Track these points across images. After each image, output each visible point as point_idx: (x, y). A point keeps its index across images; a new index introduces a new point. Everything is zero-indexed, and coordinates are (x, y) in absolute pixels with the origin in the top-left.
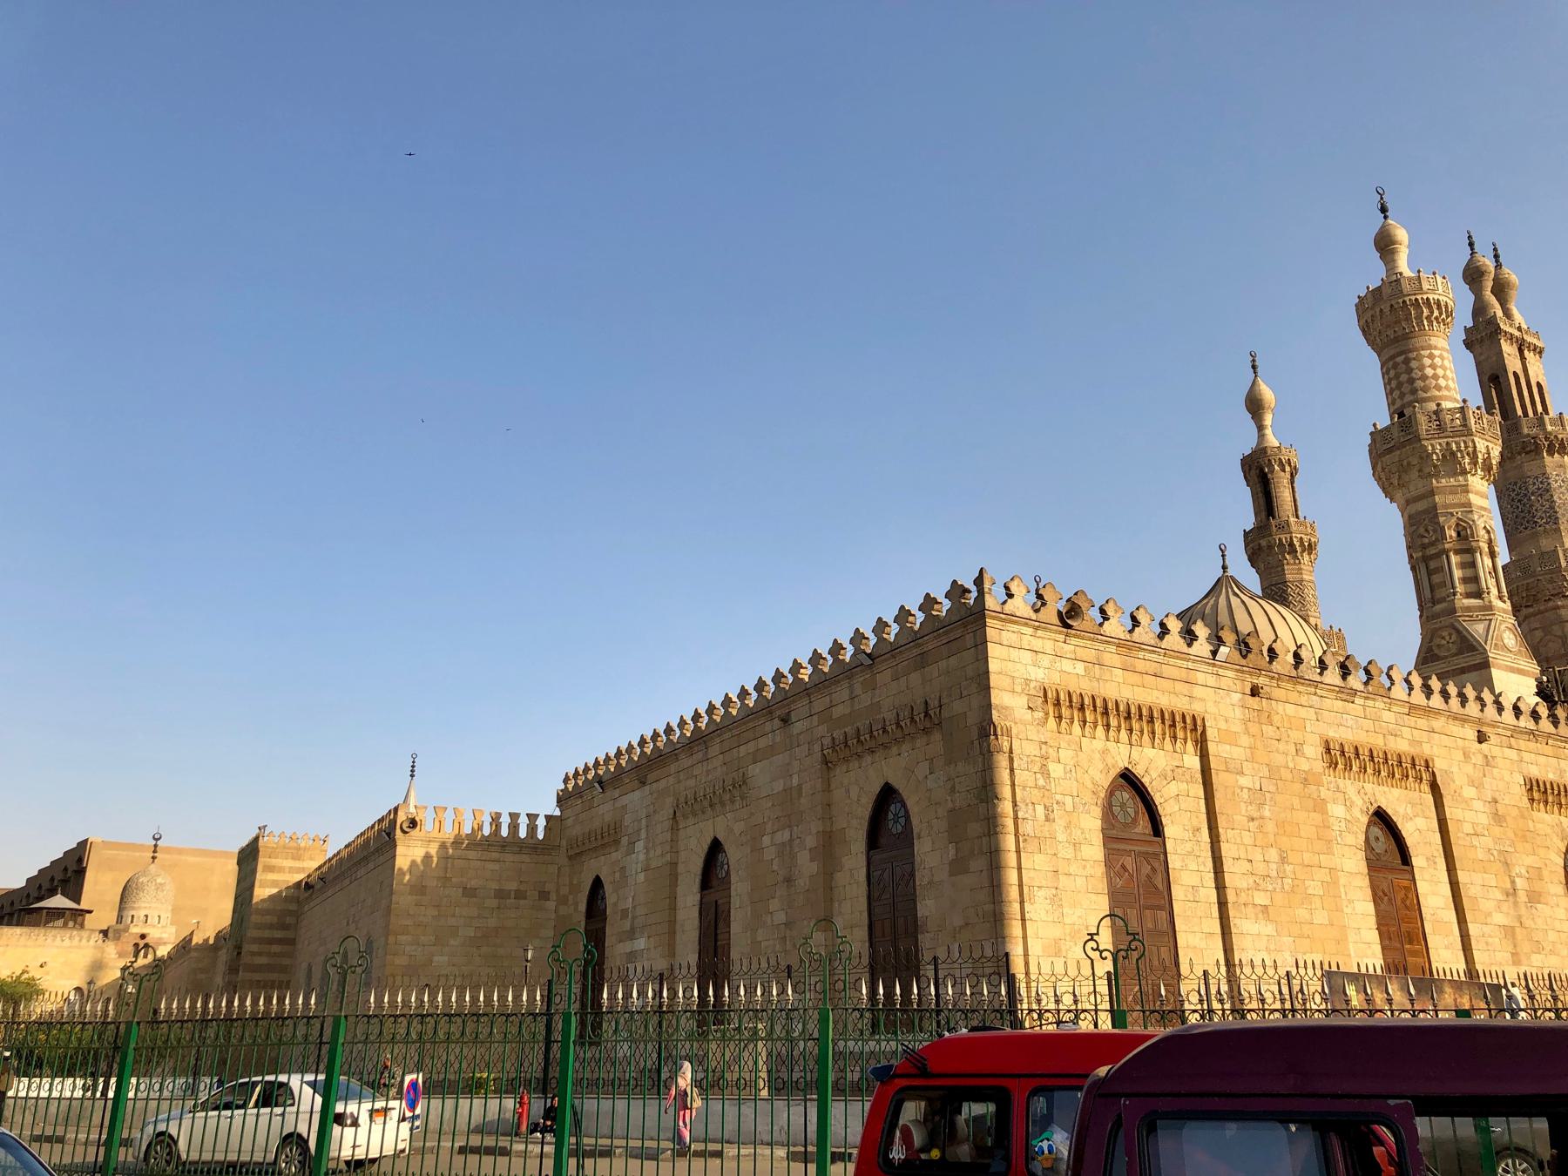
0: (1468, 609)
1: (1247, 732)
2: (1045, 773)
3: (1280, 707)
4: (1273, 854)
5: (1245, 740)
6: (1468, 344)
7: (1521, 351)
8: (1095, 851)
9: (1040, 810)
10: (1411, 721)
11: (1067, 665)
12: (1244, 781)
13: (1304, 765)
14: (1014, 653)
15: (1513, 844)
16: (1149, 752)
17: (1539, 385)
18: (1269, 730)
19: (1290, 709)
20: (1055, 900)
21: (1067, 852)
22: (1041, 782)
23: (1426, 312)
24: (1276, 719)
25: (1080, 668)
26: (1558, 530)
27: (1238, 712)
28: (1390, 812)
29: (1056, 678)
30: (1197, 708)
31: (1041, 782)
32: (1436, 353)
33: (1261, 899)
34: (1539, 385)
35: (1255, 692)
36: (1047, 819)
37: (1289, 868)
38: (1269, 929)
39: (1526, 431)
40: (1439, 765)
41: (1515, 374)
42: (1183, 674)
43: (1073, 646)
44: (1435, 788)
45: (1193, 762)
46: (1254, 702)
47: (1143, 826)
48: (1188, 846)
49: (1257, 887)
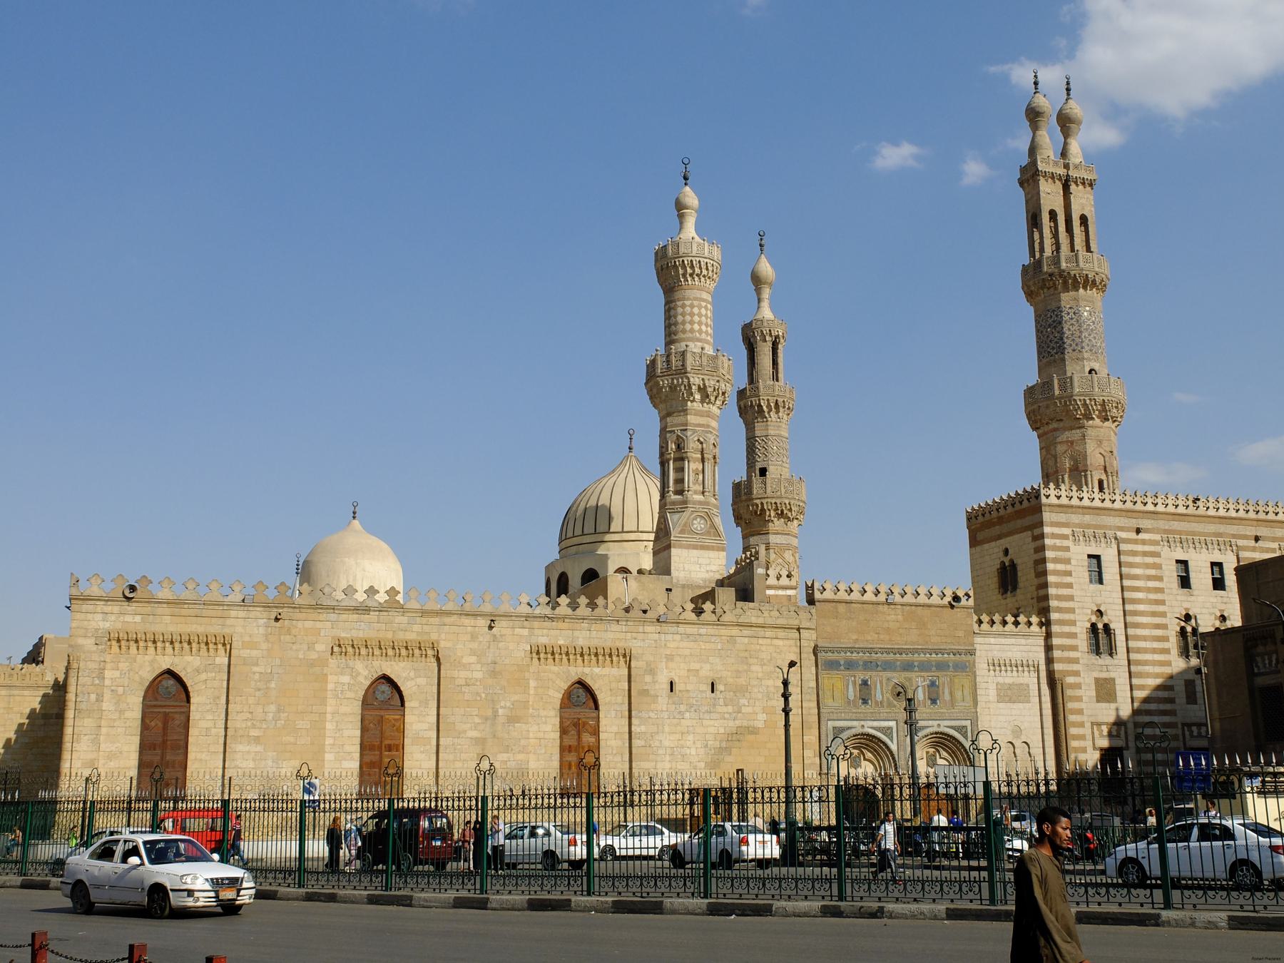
0: (674, 503)
1: (267, 640)
2: (101, 677)
3: (300, 624)
4: (273, 708)
5: (264, 646)
6: (1021, 183)
7: (1066, 187)
8: (135, 714)
9: (93, 697)
10: (424, 620)
11: (129, 618)
12: (255, 669)
13: (314, 656)
14: (90, 616)
15: (503, 688)
16: (189, 658)
17: (1084, 220)
18: (288, 638)
19: (309, 624)
20: (96, 742)
21: (116, 716)
22: (97, 682)
23: (681, 271)
24: (293, 631)
25: (138, 619)
26: (1063, 360)
27: (262, 630)
28: (392, 676)
29: (119, 626)
30: (227, 631)
31: (97, 682)
32: (688, 303)
33: (254, 733)
34: (1084, 220)
35: (277, 619)
36: (97, 700)
37: (283, 715)
38: (259, 748)
39: (1045, 269)
40: (442, 644)
41: (1053, 215)
42: (219, 613)
43: (133, 607)
44: (438, 659)
45: (222, 660)
46: (278, 624)
47: (183, 696)
48: (208, 707)
49: (254, 726)
